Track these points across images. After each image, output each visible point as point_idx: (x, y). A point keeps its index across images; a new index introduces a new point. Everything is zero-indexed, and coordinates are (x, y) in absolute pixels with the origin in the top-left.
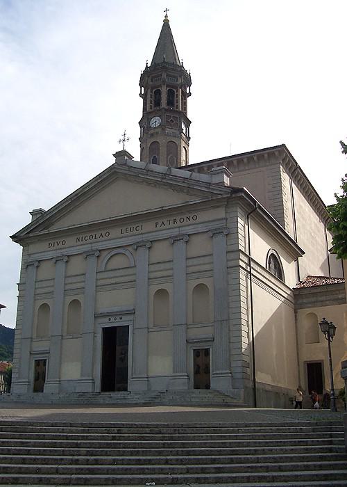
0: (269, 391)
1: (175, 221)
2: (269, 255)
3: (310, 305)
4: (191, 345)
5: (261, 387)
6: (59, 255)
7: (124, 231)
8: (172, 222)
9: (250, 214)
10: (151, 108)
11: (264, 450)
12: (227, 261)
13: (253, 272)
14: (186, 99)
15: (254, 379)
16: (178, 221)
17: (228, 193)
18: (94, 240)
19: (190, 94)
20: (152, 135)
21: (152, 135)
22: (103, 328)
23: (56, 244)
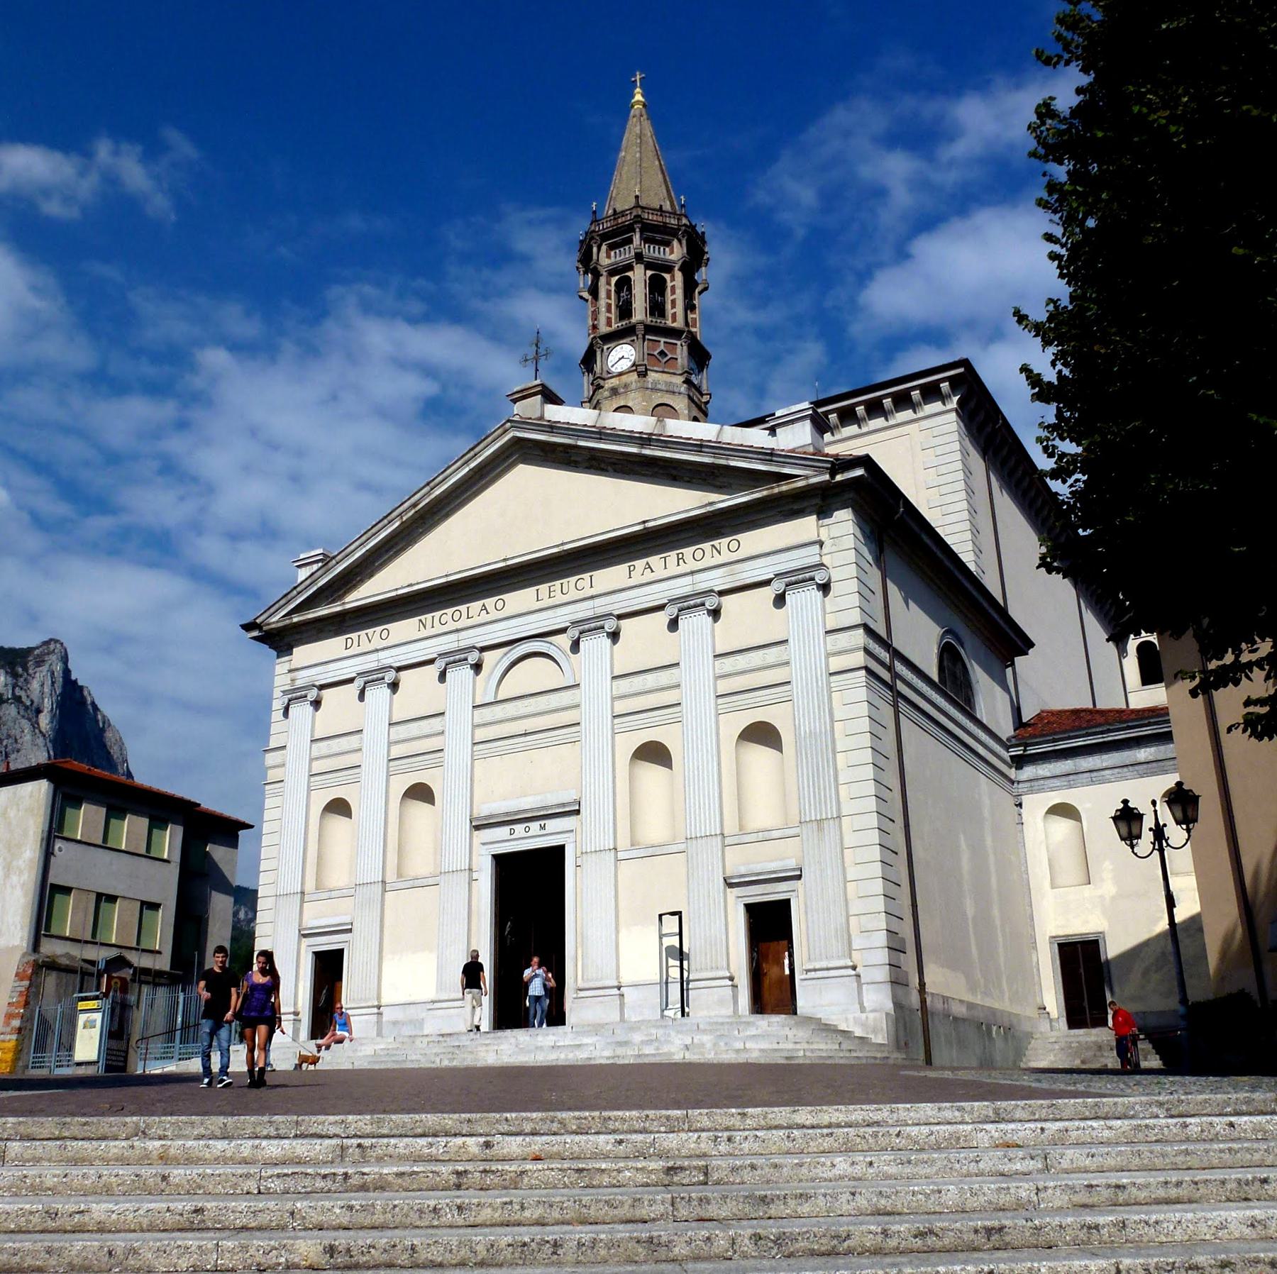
0: (964, 1020)
3: (1057, 782)
4: (737, 891)
10: (609, 323)
12: (828, 655)
13: (900, 686)
15: (922, 985)
17: (820, 470)
20: (614, 392)
21: (614, 392)
22: (497, 858)
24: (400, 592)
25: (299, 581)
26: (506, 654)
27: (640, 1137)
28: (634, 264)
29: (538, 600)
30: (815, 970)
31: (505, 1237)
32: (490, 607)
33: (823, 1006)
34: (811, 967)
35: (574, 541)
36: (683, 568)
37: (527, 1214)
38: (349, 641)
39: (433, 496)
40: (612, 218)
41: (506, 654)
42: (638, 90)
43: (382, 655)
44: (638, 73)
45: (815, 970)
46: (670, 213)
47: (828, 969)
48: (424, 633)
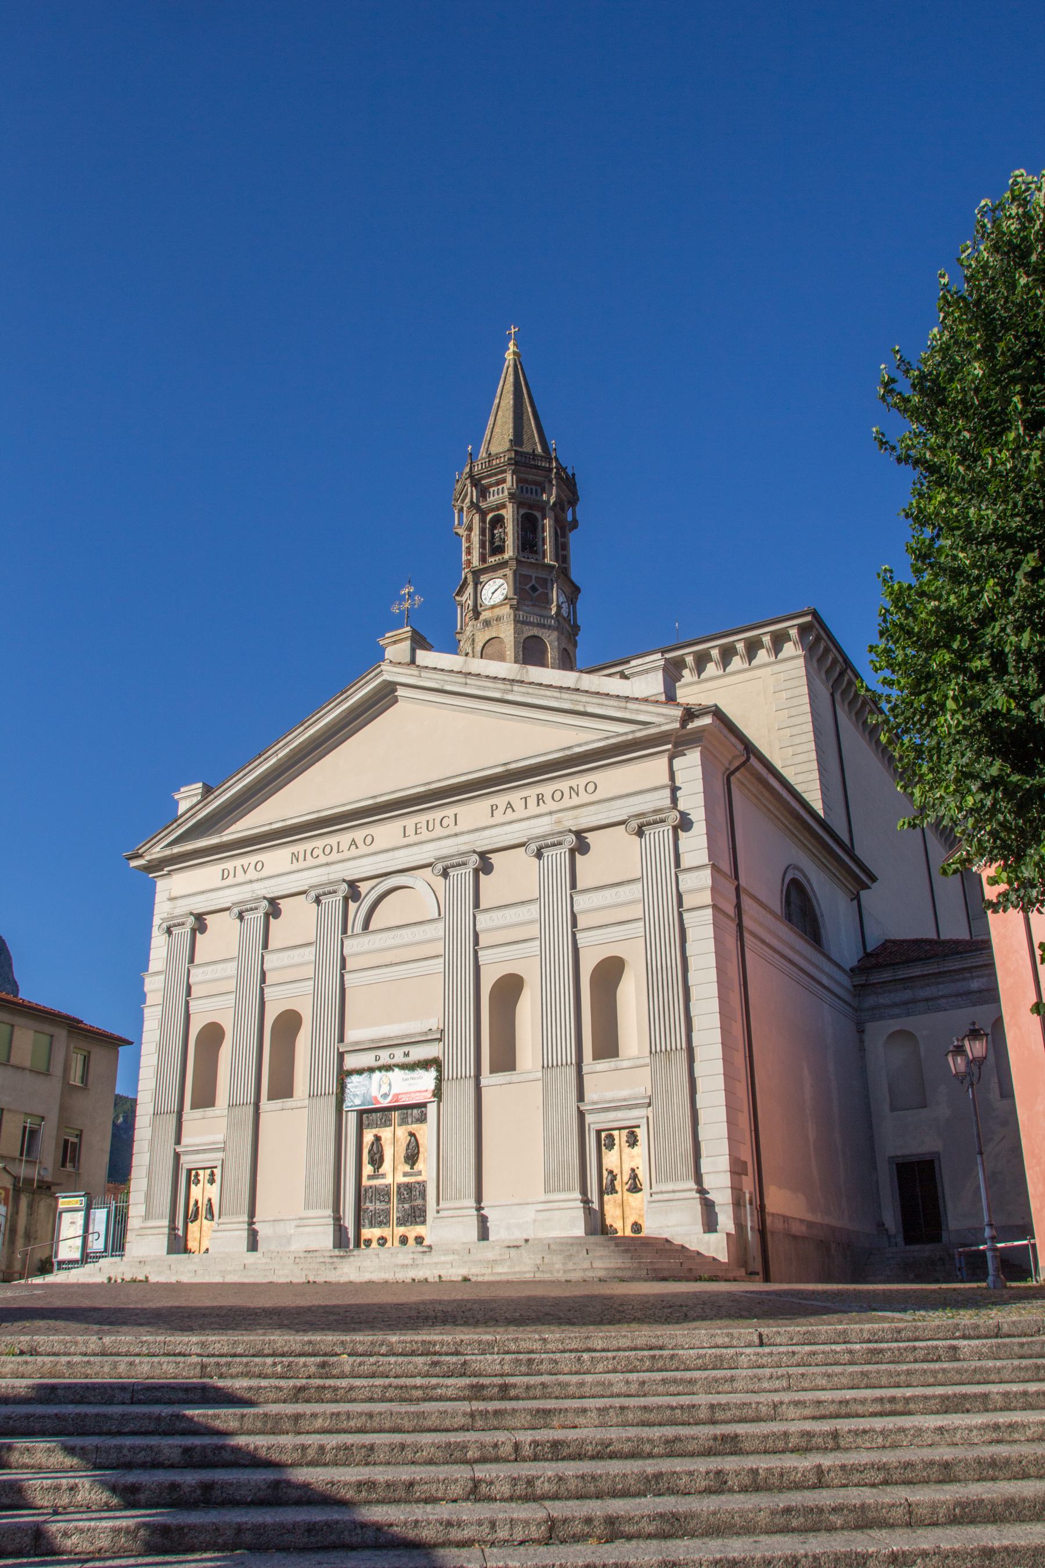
0: (803, 1238)
1: (540, 798)
2: (787, 881)
3: (897, 1011)
5: (779, 1225)
6: (247, 896)
7: (411, 830)
8: (532, 802)
9: (733, 773)
10: (483, 559)
11: (835, 1435)
14: (564, 535)
16: (548, 798)
18: (335, 856)
19: (574, 524)
20: (487, 623)
21: (487, 623)
23: (239, 870)
25: (180, 812)
27: (454, 1359)
30: (662, 1192)
31: (332, 1441)
32: (360, 843)
34: (658, 1190)
35: (439, 781)
36: (543, 808)
37: (352, 1423)
38: (226, 872)
39: (307, 735)
42: (512, 342)
43: (255, 886)
45: (662, 1192)
47: (674, 1192)
48: (296, 866)
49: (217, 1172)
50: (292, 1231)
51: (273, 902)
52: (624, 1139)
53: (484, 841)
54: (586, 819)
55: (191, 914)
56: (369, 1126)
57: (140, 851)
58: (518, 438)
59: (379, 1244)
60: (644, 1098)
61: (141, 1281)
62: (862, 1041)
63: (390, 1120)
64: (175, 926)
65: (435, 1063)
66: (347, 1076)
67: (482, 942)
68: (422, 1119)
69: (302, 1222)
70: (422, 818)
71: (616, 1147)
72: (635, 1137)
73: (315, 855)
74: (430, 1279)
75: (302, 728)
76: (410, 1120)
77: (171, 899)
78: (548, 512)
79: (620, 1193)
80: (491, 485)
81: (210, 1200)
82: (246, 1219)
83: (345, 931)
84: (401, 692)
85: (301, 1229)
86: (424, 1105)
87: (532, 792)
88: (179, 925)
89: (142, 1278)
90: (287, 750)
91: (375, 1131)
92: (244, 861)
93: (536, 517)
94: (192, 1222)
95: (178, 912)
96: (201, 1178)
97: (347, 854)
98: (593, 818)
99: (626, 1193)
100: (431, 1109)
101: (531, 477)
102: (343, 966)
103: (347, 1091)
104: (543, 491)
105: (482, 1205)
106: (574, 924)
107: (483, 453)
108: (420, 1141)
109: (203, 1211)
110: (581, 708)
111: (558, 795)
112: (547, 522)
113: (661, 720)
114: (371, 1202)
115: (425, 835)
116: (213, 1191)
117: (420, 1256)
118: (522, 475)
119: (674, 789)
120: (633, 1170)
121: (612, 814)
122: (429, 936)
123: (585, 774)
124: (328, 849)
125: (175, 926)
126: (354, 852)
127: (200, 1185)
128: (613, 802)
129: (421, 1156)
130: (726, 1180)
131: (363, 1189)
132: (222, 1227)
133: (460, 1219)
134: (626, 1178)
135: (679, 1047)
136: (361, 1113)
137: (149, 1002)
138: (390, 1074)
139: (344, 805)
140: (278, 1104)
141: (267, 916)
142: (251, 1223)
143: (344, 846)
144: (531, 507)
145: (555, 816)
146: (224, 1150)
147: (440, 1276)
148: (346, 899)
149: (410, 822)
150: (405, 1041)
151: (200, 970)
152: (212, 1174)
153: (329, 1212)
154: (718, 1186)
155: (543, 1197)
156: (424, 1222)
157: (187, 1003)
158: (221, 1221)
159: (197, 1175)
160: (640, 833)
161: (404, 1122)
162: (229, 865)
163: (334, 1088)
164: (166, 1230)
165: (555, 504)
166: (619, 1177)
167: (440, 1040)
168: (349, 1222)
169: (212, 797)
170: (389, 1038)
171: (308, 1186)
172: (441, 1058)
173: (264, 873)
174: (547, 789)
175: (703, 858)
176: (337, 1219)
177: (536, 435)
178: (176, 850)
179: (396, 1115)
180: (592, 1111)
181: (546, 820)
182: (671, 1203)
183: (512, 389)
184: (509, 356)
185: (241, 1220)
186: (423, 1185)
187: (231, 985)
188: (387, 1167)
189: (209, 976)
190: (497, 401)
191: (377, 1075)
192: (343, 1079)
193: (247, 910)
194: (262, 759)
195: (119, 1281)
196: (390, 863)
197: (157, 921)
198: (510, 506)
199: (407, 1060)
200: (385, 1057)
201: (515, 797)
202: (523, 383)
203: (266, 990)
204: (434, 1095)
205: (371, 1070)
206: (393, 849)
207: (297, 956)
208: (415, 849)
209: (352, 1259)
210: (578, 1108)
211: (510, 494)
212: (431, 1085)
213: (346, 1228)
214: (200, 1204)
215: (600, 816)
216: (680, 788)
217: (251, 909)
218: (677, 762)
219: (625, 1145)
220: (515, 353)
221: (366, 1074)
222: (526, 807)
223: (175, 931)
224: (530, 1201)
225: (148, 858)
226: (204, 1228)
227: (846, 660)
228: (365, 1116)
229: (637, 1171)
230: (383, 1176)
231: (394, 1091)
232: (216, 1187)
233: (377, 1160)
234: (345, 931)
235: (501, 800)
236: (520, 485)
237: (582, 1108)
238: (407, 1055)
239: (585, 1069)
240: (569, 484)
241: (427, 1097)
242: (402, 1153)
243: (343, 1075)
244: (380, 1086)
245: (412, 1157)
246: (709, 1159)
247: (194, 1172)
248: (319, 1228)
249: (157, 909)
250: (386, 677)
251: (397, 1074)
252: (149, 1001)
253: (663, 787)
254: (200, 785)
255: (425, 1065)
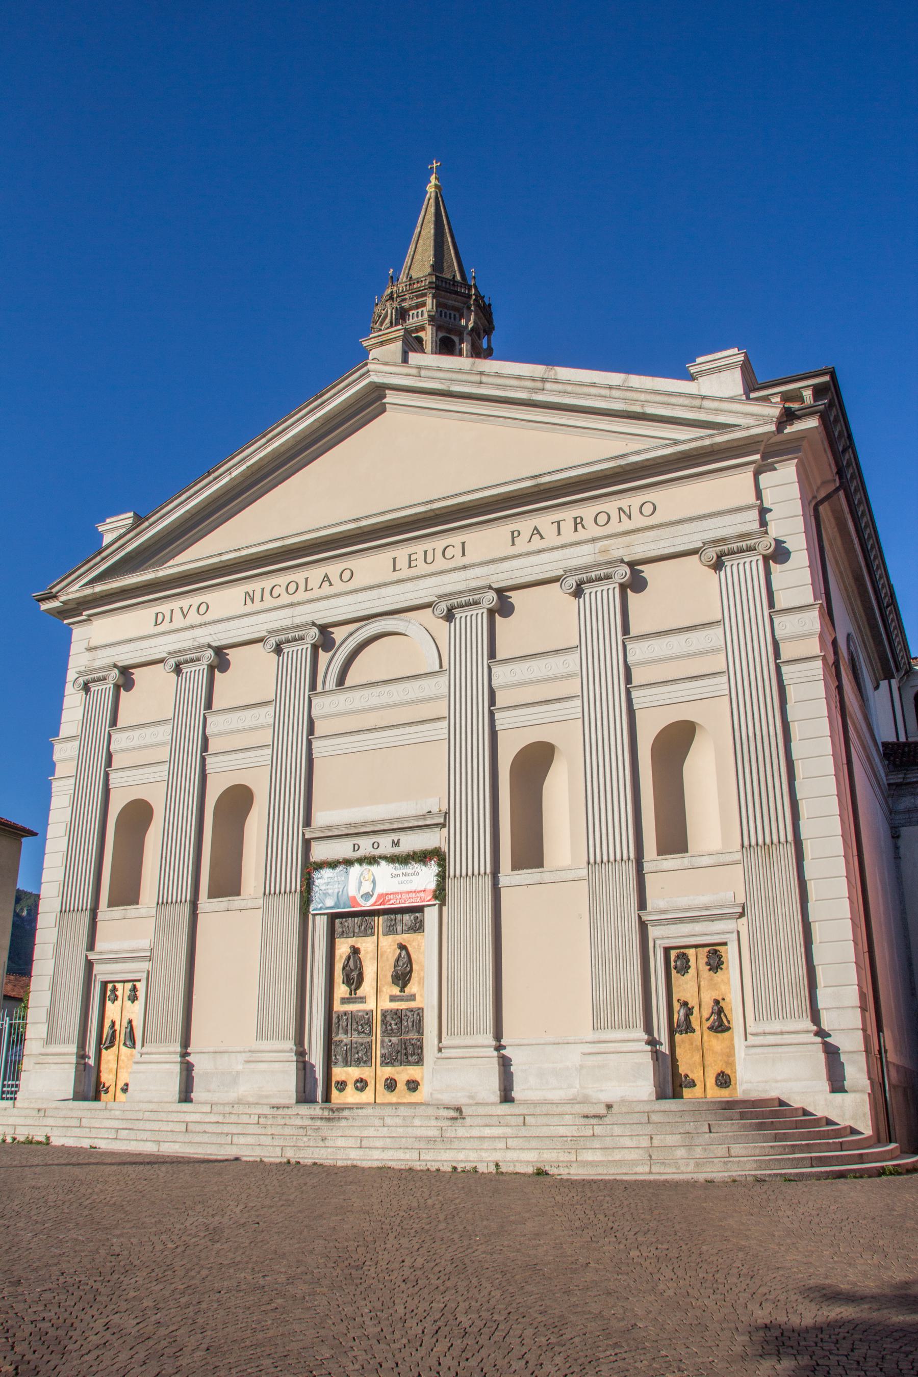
1: (578, 523)
7: (402, 563)
8: (568, 526)
16: (589, 521)
18: (301, 595)
23: (178, 615)
24: (225, 557)
26: (351, 634)
28: (427, 326)
29: (394, 570)
30: (765, 1034)
32: (335, 578)
33: (777, 1081)
34: (760, 1030)
35: (445, 498)
36: (582, 534)
39: (269, 449)
40: (408, 283)
41: (351, 634)
42: (434, 176)
43: (198, 632)
44: (434, 162)
45: (765, 1034)
46: (461, 283)
47: (782, 1033)
48: (250, 608)
49: (141, 986)
50: (240, 1067)
51: (219, 651)
52: (703, 960)
53: (502, 576)
54: (641, 547)
55: (115, 666)
56: (342, 934)
57: (54, 590)
58: (438, 265)
59: (357, 1088)
60: (734, 906)
61: (39, 1143)
62: (897, 848)
63: (373, 928)
64: (94, 681)
65: (436, 856)
66: (315, 869)
67: (500, 702)
68: (418, 927)
69: (253, 1057)
70: (418, 548)
71: (692, 971)
72: (720, 957)
73: (275, 595)
74: (482, 1168)
75: (264, 440)
76: (399, 928)
77: (90, 649)
78: (466, 337)
79: (698, 1033)
80: (411, 308)
81: (130, 1022)
82: (179, 1049)
83: (313, 687)
84: (391, 397)
85: (253, 1065)
86: (420, 909)
87: (567, 515)
88: (99, 680)
89: (42, 1139)
90: (244, 467)
91: (351, 941)
92: (184, 602)
93: (453, 341)
94: (107, 1048)
95: (98, 664)
96: (119, 993)
97: (317, 593)
98: (652, 546)
99: (706, 1033)
100: (431, 916)
101: (450, 302)
102: (311, 731)
103: (315, 889)
104: (461, 316)
105: (503, 1042)
106: (628, 679)
107: (403, 277)
108: (413, 956)
109: (121, 1036)
110: (637, 409)
111: (602, 519)
112: (464, 346)
113: (751, 421)
114: (346, 1032)
115: (422, 568)
116: (135, 1011)
117: (449, 1123)
118: (441, 300)
119: (763, 512)
120: (717, 1002)
121: (678, 541)
122: (427, 693)
123: (639, 492)
124: (292, 588)
125: (94, 681)
126: (326, 590)
127: (118, 1003)
128: (679, 527)
129: (414, 975)
130: (854, 1019)
131: (334, 1016)
132: (146, 1058)
133: (474, 1061)
134: (706, 1014)
135: (625, 857)
136: (333, 918)
137: (58, 774)
138: (374, 868)
139: (318, 530)
140: (221, 903)
141: (211, 668)
142: (185, 1054)
143: (314, 583)
144: (449, 331)
145: (599, 545)
146: (150, 959)
147: (497, 1165)
148: (315, 648)
149: (401, 553)
150: (395, 826)
151: (124, 735)
152: (134, 989)
153: (290, 1045)
154: (842, 1027)
155: (591, 1036)
156: (420, 1062)
157: (107, 775)
158: (145, 1050)
159: (115, 989)
160: (718, 565)
161: (391, 930)
162: (164, 608)
163: (297, 883)
164: (73, 1059)
165: (472, 329)
166: (696, 1011)
167: (443, 825)
168: (316, 1057)
169: (147, 524)
170: (374, 822)
171: (261, 1010)
172: (445, 849)
173: (209, 617)
174: (587, 512)
175: (806, 595)
176: (301, 1053)
177: (455, 264)
178: (99, 588)
179: (380, 922)
180: (658, 923)
181: (588, 548)
182: (780, 1049)
183: (433, 219)
184: (431, 189)
185: (172, 1049)
186: (419, 1013)
187: (164, 753)
188: (367, 988)
189: (135, 743)
190: (417, 230)
191: (356, 869)
192: (309, 873)
193: (186, 662)
194: (211, 478)
195: (9, 1140)
196: (376, 603)
197: (71, 675)
198: (429, 329)
199: (396, 851)
200: (366, 846)
201: (544, 521)
202: (443, 214)
203: (209, 760)
204: (436, 897)
205: (348, 862)
206: (379, 586)
207: (249, 718)
208: (409, 586)
209: (343, 1123)
210: (640, 917)
211: (429, 316)
212: (432, 884)
213: (313, 1066)
214: (117, 1027)
215: (662, 544)
216: (770, 510)
217: (192, 661)
218: (766, 479)
219: (704, 968)
220: (436, 186)
221: (341, 868)
222: (559, 534)
223: (94, 688)
224: (571, 1039)
225: (63, 598)
226: (122, 1057)
227: (850, 437)
228: (337, 921)
229: (722, 1004)
230: (362, 1000)
231: (380, 890)
232: (139, 1005)
233: (354, 979)
234: (313, 687)
235: (525, 525)
236: (439, 309)
237: (644, 918)
238: (396, 844)
239: (647, 867)
240: (485, 311)
241: (427, 899)
242: (388, 972)
243: (310, 868)
244: (361, 883)
245: (402, 977)
246: (829, 990)
247: (110, 986)
248: (277, 1065)
249: (72, 663)
250: (374, 378)
251: (384, 870)
252: (59, 772)
253: (749, 507)
254: (131, 514)
255: (422, 857)
